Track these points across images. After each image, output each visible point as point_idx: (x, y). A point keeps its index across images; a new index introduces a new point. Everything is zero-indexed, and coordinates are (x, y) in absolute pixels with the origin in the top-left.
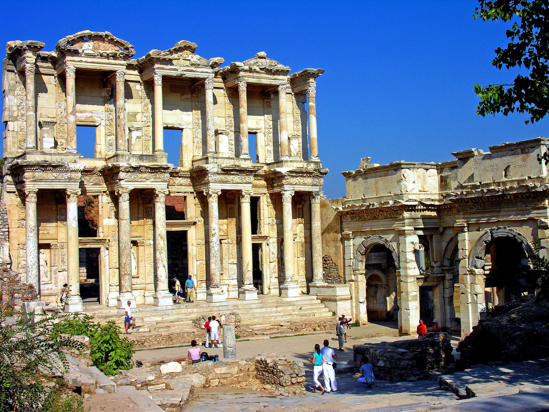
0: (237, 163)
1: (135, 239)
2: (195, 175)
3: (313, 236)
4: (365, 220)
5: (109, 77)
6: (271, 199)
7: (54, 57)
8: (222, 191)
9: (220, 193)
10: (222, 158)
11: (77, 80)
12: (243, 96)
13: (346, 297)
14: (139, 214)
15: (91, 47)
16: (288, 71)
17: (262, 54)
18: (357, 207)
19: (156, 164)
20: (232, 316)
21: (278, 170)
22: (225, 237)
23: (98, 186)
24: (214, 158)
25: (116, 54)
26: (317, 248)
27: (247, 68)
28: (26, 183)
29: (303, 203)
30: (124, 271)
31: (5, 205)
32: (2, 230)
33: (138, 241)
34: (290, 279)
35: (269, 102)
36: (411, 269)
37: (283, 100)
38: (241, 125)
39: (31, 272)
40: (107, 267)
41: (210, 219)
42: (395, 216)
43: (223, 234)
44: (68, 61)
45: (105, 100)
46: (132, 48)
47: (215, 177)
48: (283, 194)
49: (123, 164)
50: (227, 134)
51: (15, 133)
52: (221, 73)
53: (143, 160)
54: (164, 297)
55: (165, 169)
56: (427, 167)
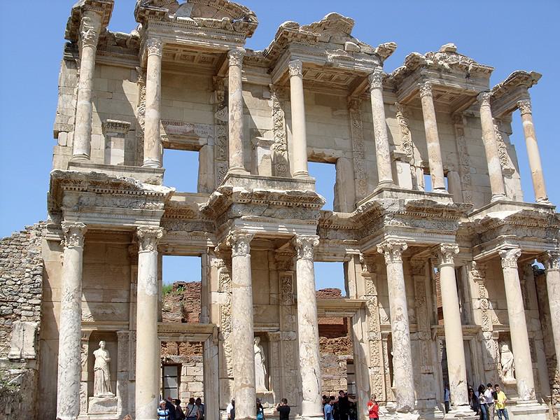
1: (263, 329)
6: (479, 269)
9: (405, 247)
14: (270, 287)
17: (451, 45)
24: (392, 190)
27: (429, 62)
28: (65, 213)
30: (241, 380)
31: (42, 261)
32: (30, 301)
35: (462, 129)
44: (150, 30)
45: (214, 108)
47: (395, 221)
48: (504, 255)
53: (273, 187)
55: (311, 200)
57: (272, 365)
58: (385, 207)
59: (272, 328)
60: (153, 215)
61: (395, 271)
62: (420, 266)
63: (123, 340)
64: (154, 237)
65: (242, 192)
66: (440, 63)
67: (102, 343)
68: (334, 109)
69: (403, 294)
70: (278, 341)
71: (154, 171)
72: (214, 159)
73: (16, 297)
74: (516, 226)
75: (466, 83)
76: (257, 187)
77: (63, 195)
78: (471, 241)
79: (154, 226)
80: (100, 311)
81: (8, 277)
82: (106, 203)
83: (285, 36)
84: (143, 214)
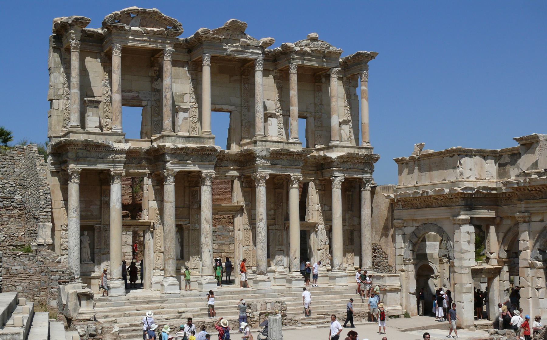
0: (286, 147)
1: (180, 223)
2: (242, 159)
3: (363, 224)
4: (417, 208)
5: (156, 56)
7: (101, 34)
8: (270, 175)
9: (268, 177)
10: (270, 141)
11: (123, 58)
12: (294, 78)
13: (397, 287)
16: (340, 53)
17: (314, 35)
18: (410, 194)
19: (203, 145)
21: (329, 154)
22: (272, 223)
24: (262, 141)
25: (163, 32)
26: (367, 236)
30: (168, 255)
32: (45, 210)
34: (338, 267)
35: (320, 86)
36: (466, 259)
37: (335, 83)
38: (291, 108)
40: (152, 251)
41: (257, 204)
42: (450, 204)
46: (180, 25)
48: (333, 180)
49: (169, 145)
50: (276, 117)
51: (59, 111)
52: (272, 55)
53: (189, 142)
54: (209, 283)
56: (484, 154)
57: (185, 244)
58: (257, 152)
60: (119, 162)
61: (261, 191)
62: (278, 188)
63: (98, 230)
64: (120, 175)
66: (306, 49)
67: (86, 233)
68: (231, 76)
69: (265, 206)
70: (189, 230)
71: (119, 135)
72: (152, 115)
73: (13, 195)
74: (343, 162)
76: (179, 143)
78: (316, 167)
79: (120, 168)
81: (6, 181)
84: (114, 162)
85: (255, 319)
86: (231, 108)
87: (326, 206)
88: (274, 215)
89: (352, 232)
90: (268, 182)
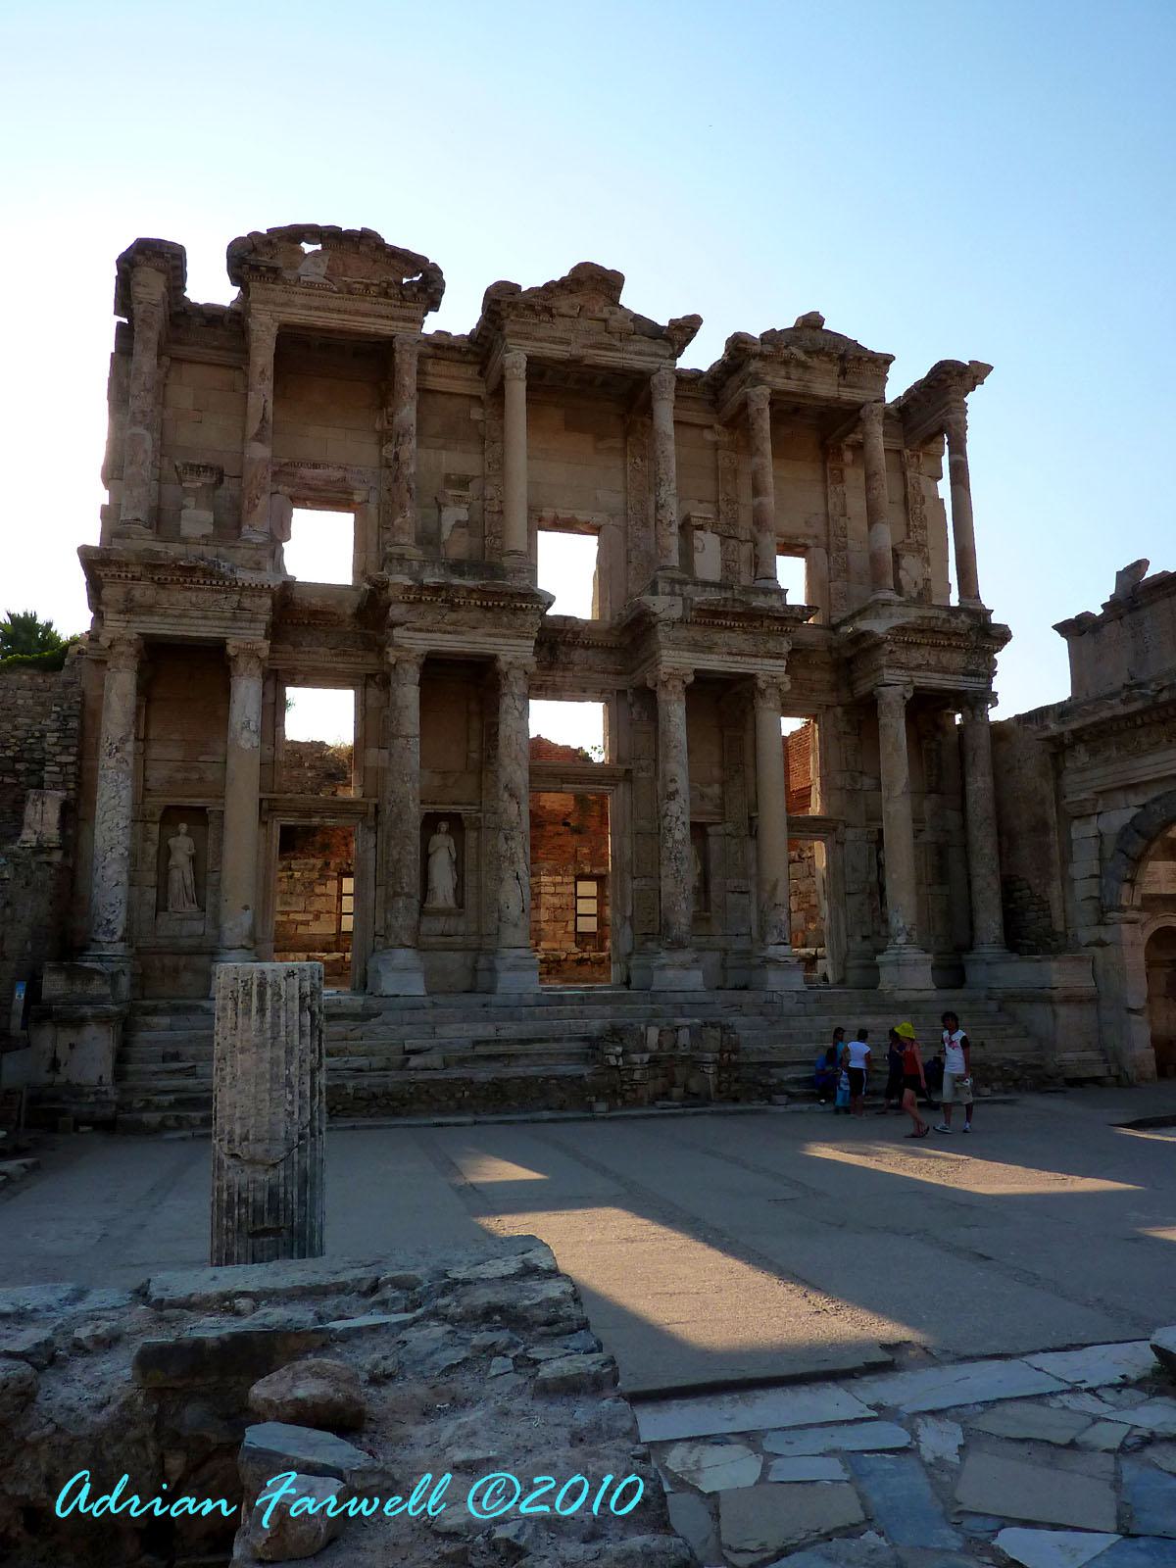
1: (453, 809)
9: (690, 679)
14: (468, 741)
15: (323, 270)
20: (717, 1033)
21: (864, 625)
22: (717, 819)
23: (353, 659)
26: (986, 851)
29: (939, 737)
33: (463, 816)
35: (841, 471)
39: (100, 870)
43: (709, 808)
44: (254, 301)
52: (707, 384)
53: (462, 575)
54: (514, 968)
58: (656, 609)
59: (469, 808)
64: (253, 654)
65: (406, 583)
67: (183, 827)
75: (839, 385)
77: (102, 587)
80: (180, 776)
82: (173, 600)
83: (496, 308)
85: (637, 1076)
86: (598, 519)
87: (864, 778)
88: (722, 799)
89: (941, 851)
90: (689, 691)
